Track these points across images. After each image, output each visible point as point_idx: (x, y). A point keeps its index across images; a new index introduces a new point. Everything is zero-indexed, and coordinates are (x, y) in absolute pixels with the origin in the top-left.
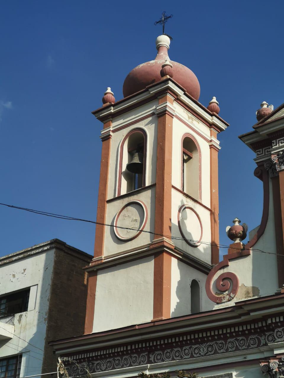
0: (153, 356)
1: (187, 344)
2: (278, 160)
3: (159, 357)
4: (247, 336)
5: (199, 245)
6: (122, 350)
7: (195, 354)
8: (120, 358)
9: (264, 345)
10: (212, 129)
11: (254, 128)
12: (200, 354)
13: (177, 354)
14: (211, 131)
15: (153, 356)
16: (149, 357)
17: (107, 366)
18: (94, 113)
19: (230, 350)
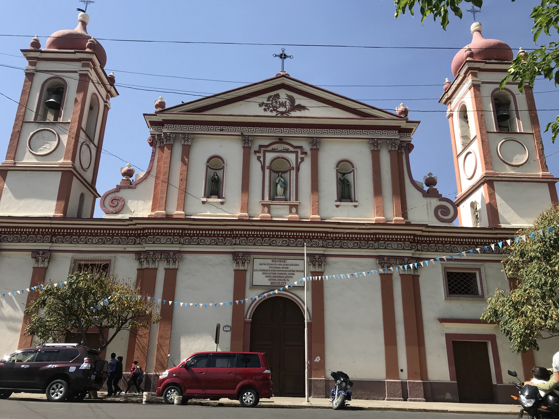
0: (55, 238)
1: (84, 235)
2: (166, 137)
3: (60, 240)
4: (128, 237)
5: (86, 171)
6: (30, 230)
7: (88, 242)
8: (26, 236)
9: (138, 244)
10: (109, 94)
11: (155, 113)
12: (92, 242)
13: (75, 240)
14: (107, 95)
15: (55, 238)
16: (51, 239)
17: (13, 239)
18: (22, 51)
19: (115, 243)
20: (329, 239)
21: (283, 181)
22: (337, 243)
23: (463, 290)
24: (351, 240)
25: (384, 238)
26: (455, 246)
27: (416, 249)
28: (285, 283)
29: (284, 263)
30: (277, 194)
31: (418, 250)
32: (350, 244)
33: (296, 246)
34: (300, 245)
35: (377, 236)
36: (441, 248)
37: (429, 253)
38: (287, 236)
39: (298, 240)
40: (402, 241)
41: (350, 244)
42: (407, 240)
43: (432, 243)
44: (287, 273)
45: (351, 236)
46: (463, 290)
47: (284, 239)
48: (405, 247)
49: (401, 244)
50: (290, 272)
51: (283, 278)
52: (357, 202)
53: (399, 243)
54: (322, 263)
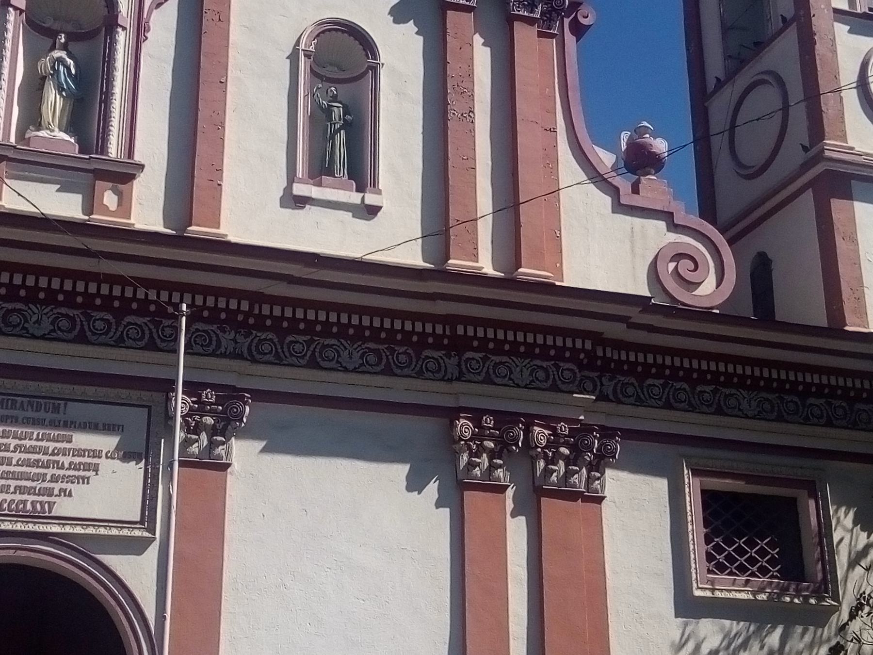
20: (263, 328)
21: (73, 71)
22: (298, 347)
23: (752, 561)
24: (353, 339)
25: (485, 340)
26: (733, 391)
27: (597, 392)
28: (51, 505)
29: (55, 415)
30: (40, 124)
31: (602, 397)
32: (350, 355)
33: (119, 343)
34: (134, 340)
35: (460, 330)
36: (682, 396)
37: (641, 411)
38: (79, 299)
39: (129, 319)
40: (548, 358)
41: (350, 355)
42: (567, 354)
43: (656, 376)
44: (66, 460)
45: (355, 320)
46: (752, 561)
47: (63, 310)
48: (559, 382)
49: (546, 370)
50: (77, 460)
51: (38, 485)
52: (379, 192)
53: (538, 362)
54: (225, 428)
